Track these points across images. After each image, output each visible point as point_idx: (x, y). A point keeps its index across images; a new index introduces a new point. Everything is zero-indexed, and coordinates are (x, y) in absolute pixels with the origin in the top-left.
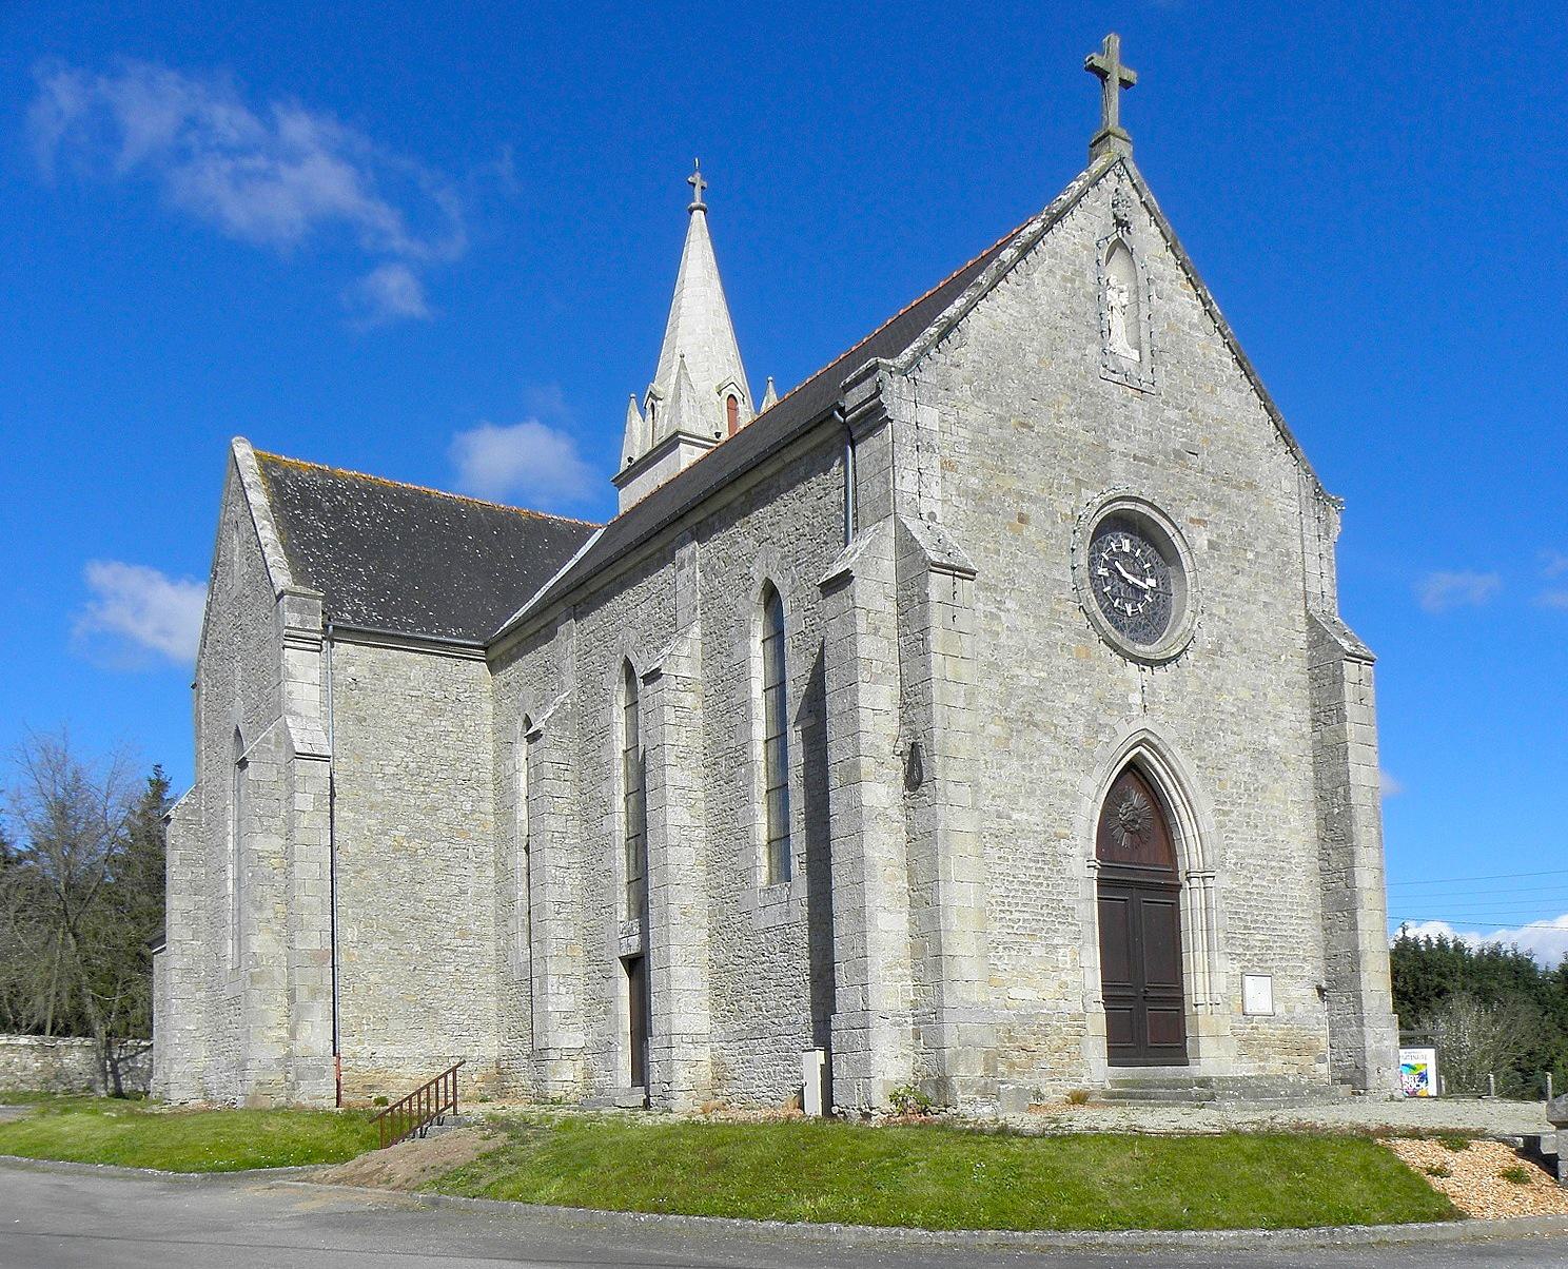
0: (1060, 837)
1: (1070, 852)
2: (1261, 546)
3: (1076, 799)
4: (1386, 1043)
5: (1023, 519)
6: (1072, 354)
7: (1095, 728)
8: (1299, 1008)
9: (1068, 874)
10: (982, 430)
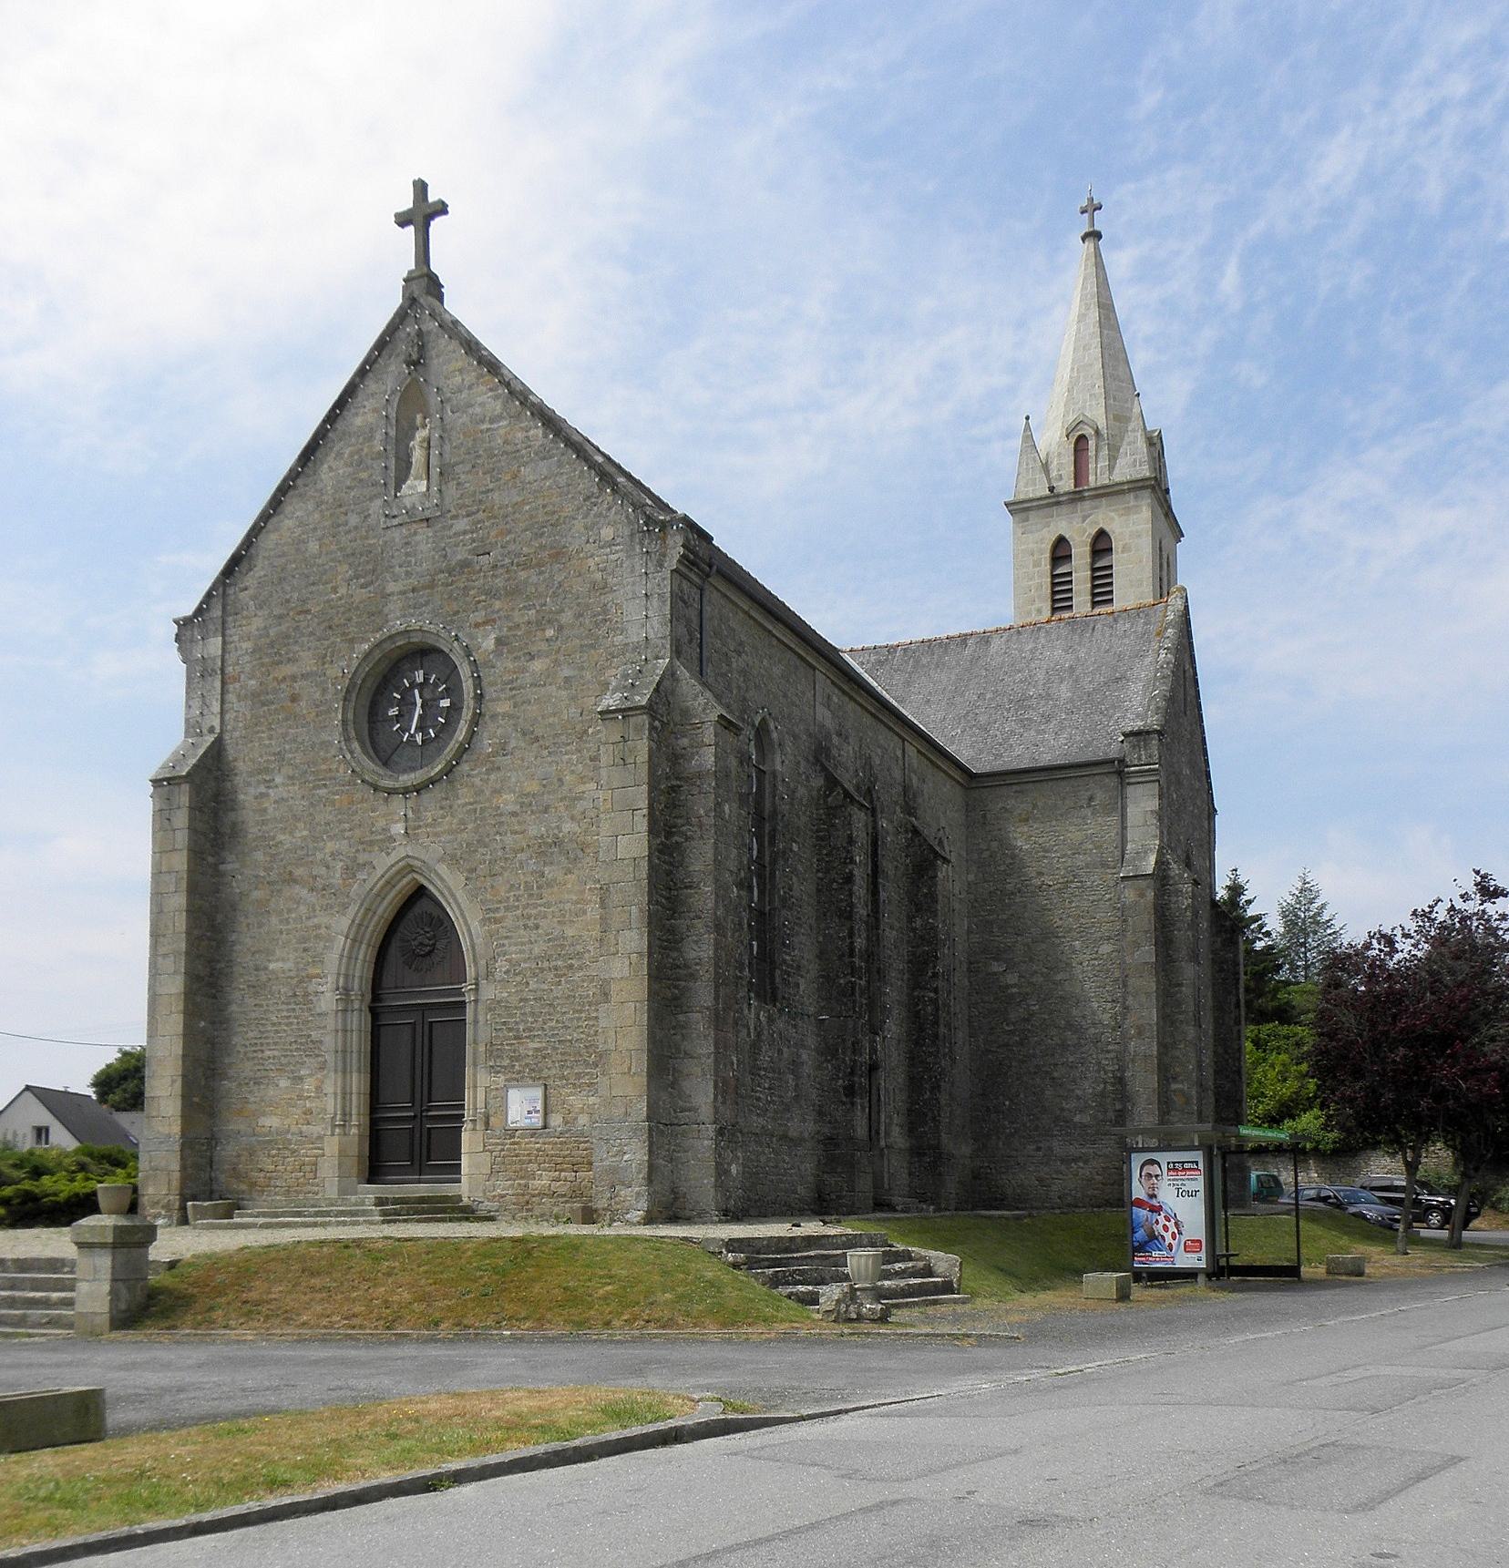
0: (310, 977)
1: (321, 989)
2: (567, 617)
4: (626, 1157)
7: (351, 871)
8: (583, 1120)
9: (319, 1011)
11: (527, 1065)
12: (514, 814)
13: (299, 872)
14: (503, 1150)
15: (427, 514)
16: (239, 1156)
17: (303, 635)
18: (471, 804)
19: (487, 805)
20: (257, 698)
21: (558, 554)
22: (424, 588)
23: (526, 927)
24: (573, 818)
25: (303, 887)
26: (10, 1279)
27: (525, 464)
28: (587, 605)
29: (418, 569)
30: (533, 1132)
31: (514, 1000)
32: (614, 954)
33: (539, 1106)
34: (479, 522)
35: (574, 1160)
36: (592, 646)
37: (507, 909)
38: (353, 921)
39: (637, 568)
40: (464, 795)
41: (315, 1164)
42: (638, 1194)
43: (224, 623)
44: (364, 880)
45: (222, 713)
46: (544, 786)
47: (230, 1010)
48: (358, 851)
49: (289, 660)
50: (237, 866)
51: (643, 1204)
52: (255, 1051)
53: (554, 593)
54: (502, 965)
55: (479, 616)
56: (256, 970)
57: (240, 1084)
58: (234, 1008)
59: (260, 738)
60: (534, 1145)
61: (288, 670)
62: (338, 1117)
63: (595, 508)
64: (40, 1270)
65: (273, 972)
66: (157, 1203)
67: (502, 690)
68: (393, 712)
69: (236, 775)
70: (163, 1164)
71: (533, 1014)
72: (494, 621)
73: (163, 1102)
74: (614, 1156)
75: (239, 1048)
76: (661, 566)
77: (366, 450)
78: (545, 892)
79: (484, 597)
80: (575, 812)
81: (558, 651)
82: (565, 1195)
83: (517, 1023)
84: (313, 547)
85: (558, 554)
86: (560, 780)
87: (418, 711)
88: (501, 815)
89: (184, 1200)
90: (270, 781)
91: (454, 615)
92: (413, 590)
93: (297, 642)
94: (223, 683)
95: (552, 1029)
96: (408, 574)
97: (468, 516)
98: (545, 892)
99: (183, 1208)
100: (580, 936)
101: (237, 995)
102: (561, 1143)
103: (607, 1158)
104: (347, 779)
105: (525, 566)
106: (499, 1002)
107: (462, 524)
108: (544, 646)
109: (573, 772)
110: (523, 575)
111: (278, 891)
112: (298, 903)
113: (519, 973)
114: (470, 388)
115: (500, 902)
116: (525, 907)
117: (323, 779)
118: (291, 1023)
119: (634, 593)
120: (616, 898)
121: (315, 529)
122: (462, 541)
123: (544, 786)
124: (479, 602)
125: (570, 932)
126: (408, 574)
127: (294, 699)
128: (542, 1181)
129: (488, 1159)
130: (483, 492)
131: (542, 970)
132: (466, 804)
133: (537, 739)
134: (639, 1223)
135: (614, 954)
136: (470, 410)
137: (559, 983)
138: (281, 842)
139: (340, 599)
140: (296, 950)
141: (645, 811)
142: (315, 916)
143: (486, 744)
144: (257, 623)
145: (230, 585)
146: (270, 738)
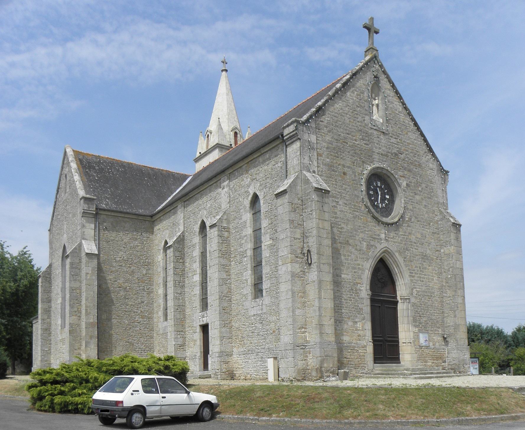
0: (358, 283)
2: (424, 186)
3: (363, 270)
4: (466, 356)
5: (345, 174)
6: (360, 119)
7: (369, 247)
9: (360, 297)
10: (330, 143)
12: (415, 243)
36: (430, 198)
37: (415, 273)
59: (332, 184)
61: (342, 162)
66: (328, 371)
71: (423, 309)
92: (382, 154)
95: (429, 315)
110: (412, 167)
117: (357, 209)
138: (343, 228)
140: (352, 272)
146: (336, 185)
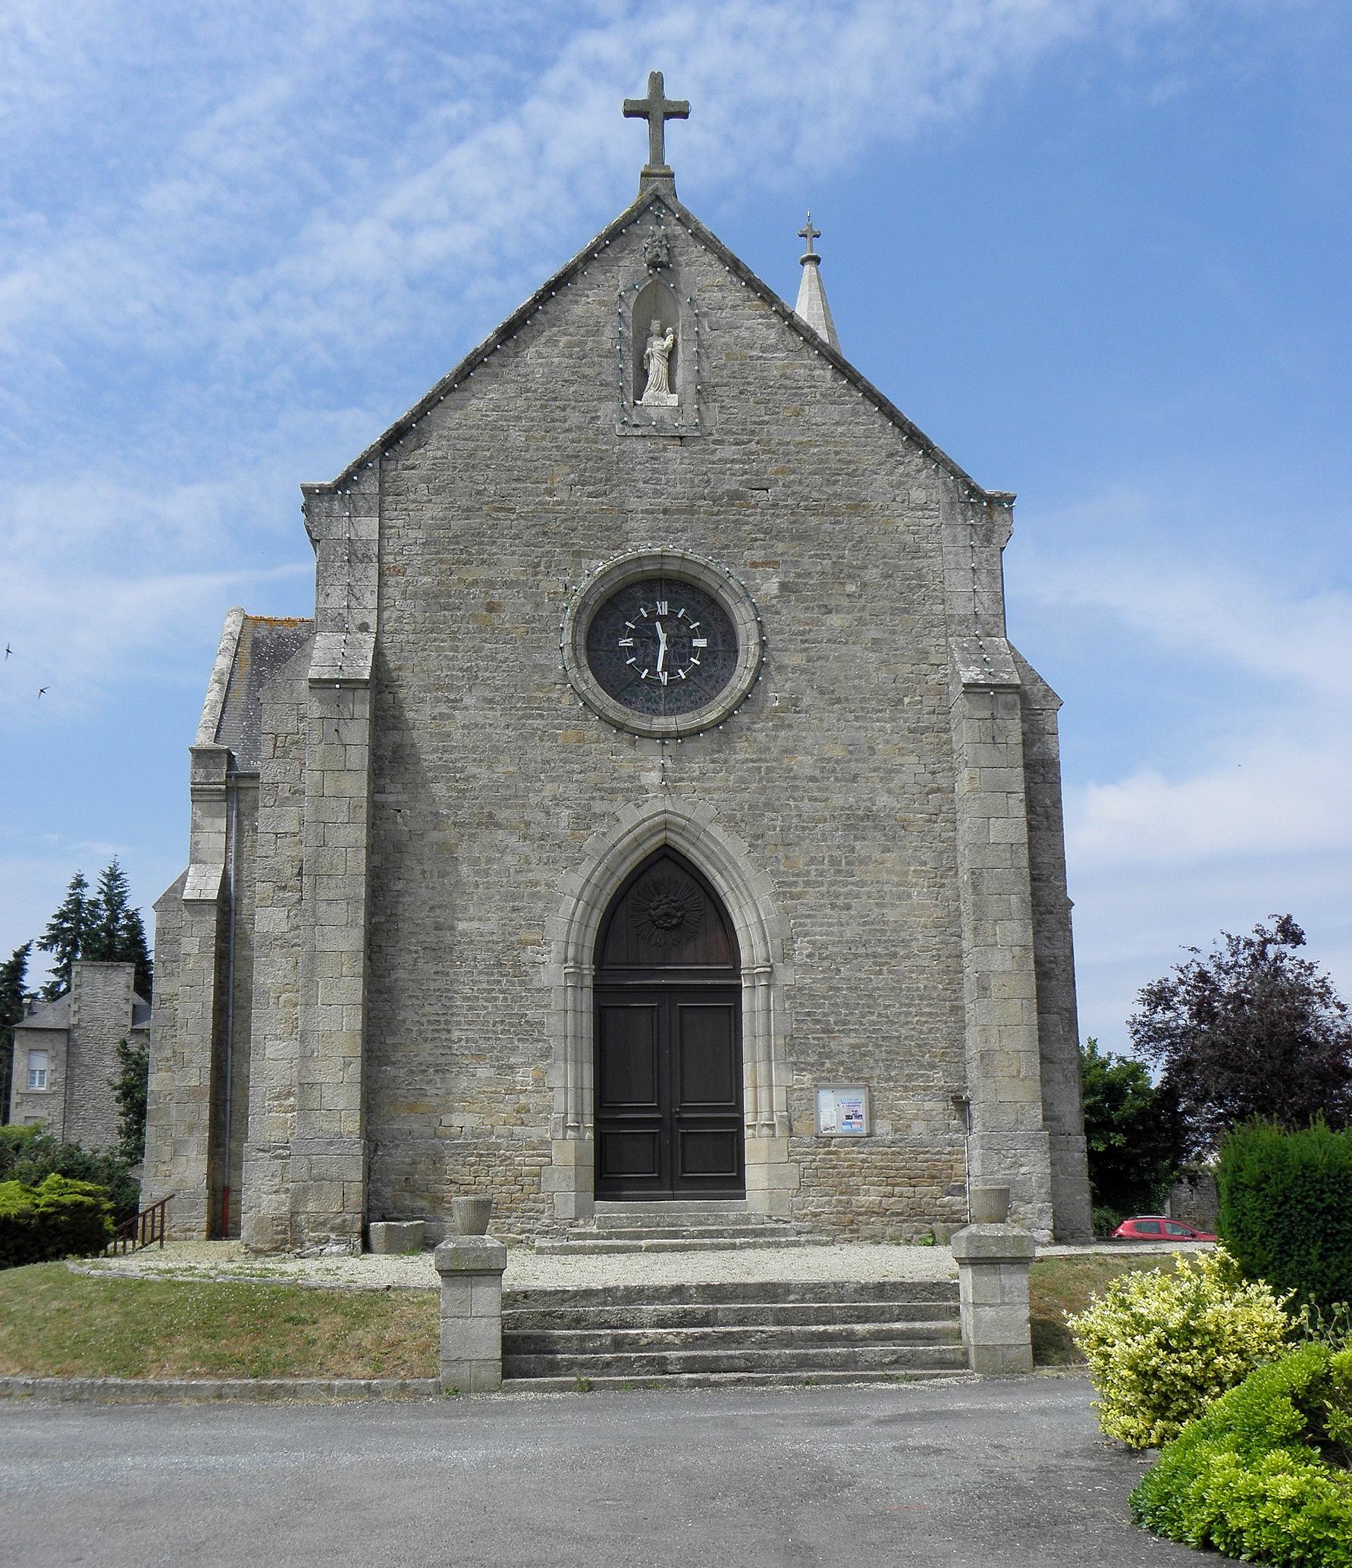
1: (540, 958)
2: (872, 574)
3: (552, 902)
4: (1023, 1170)
5: (491, 608)
6: (575, 418)
7: (584, 820)
8: (919, 1128)
9: (536, 984)
10: (444, 524)
11: (841, 1063)
12: (813, 779)
13: (502, 815)
14: (814, 1160)
15: (683, 432)
16: (414, 1163)
17: (503, 536)
18: (753, 761)
19: (774, 764)
20: (436, 599)
21: (858, 506)
22: (679, 511)
23: (833, 906)
24: (889, 792)
25: (511, 834)
26: (735, 1310)
27: (810, 404)
28: (897, 567)
29: (671, 490)
30: (856, 1140)
31: (821, 988)
32: (992, 946)
33: (862, 1110)
34: (753, 453)
35: (912, 1174)
36: (905, 611)
37: (807, 884)
38: (588, 881)
39: (960, 537)
40: (742, 751)
41: (539, 1175)
42: (1041, 1211)
43: (381, 502)
44: (604, 834)
45: (380, 609)
46: (851, 752)
47: (393, 977)
48: (593, 798)
49: (483, 562)
50: (404, 797)
51: (1048, 1222)
52: (438, 1031)
53: (854, 546)
54: (802, 946)
55: (758, 555)
56: (437, 929)
57: (412, 1072)
58: (401, 974)
59: (439, 649)
60: (857, 1154)
61: (483, 573)
62: (570, 1117)
63: (902, 467)
64: (745, 1298)
65: (464, 934)
66: (323, 1224)
67: (791, 640)
68: (626, 642)
69: (400, 686)
70: (334, 1171)
71: (847, 1005)
72: (777, 563)
73: (327, 1092)
74: (1009, 1169)
75: (408, 1025)
76: (989, 541)
77: (590, 345)
78: (857, 869)
79: (762, 536)
80: (892, 785)
81: (863, 609)
82: (901, 1214)
83: (825, 1015)
84: (517, 437)
85: (857, 507)
86: (871, 748)
87: (663, 648)
88: (795, 778)
89: (368, 1217)
90: (455, 701)
91: (723, 549)
92: (665, 512)
93: (494, 543)
94: (381, 575)
95: (874, 1023)
96: (656, 492)
97: (737, 444)
98: (857, 869)
99: (365, 1234)
100: (905, 922)
101: (407, 959)
102: (893, 1153)
103: (998, 1171)
104: (574, 712)
105: (814, 511)
106: (800, 989)
107: (727, 451)
108: (845, 602)
109: (887, 742)
110: (814, 521)
111: (471, 835)
112: (503, 852)
113: (826, 958)
114: (734, 307)
115: (798, 875)
116: (832, 884)
117: (538, 708)
118: (495, 999)
119: (957, 563)
120: (989, 885)
121: (518, 418)
122: (729, 469)
123: (851, 752)
124: (756, 540)
125: (892, 916)
126: (657, 493)
127: (491, 608)
128: (870, 1197)
129: (795, 1171)
130: (756, 423)
131: (856, 956)
132: (747, 760)
133: (838, 701)
134: (1050, 1243)
135: (992, 946)
136: (735, 332)
137: (880, 972)
138: (474, 776)
139: (559, 503)
140: (501, 909)
141: (1022, 796)
142: (531, 871)
143: (774, 696)
144: (432, 512)
145: (389, 459)
146: (455, 649)
